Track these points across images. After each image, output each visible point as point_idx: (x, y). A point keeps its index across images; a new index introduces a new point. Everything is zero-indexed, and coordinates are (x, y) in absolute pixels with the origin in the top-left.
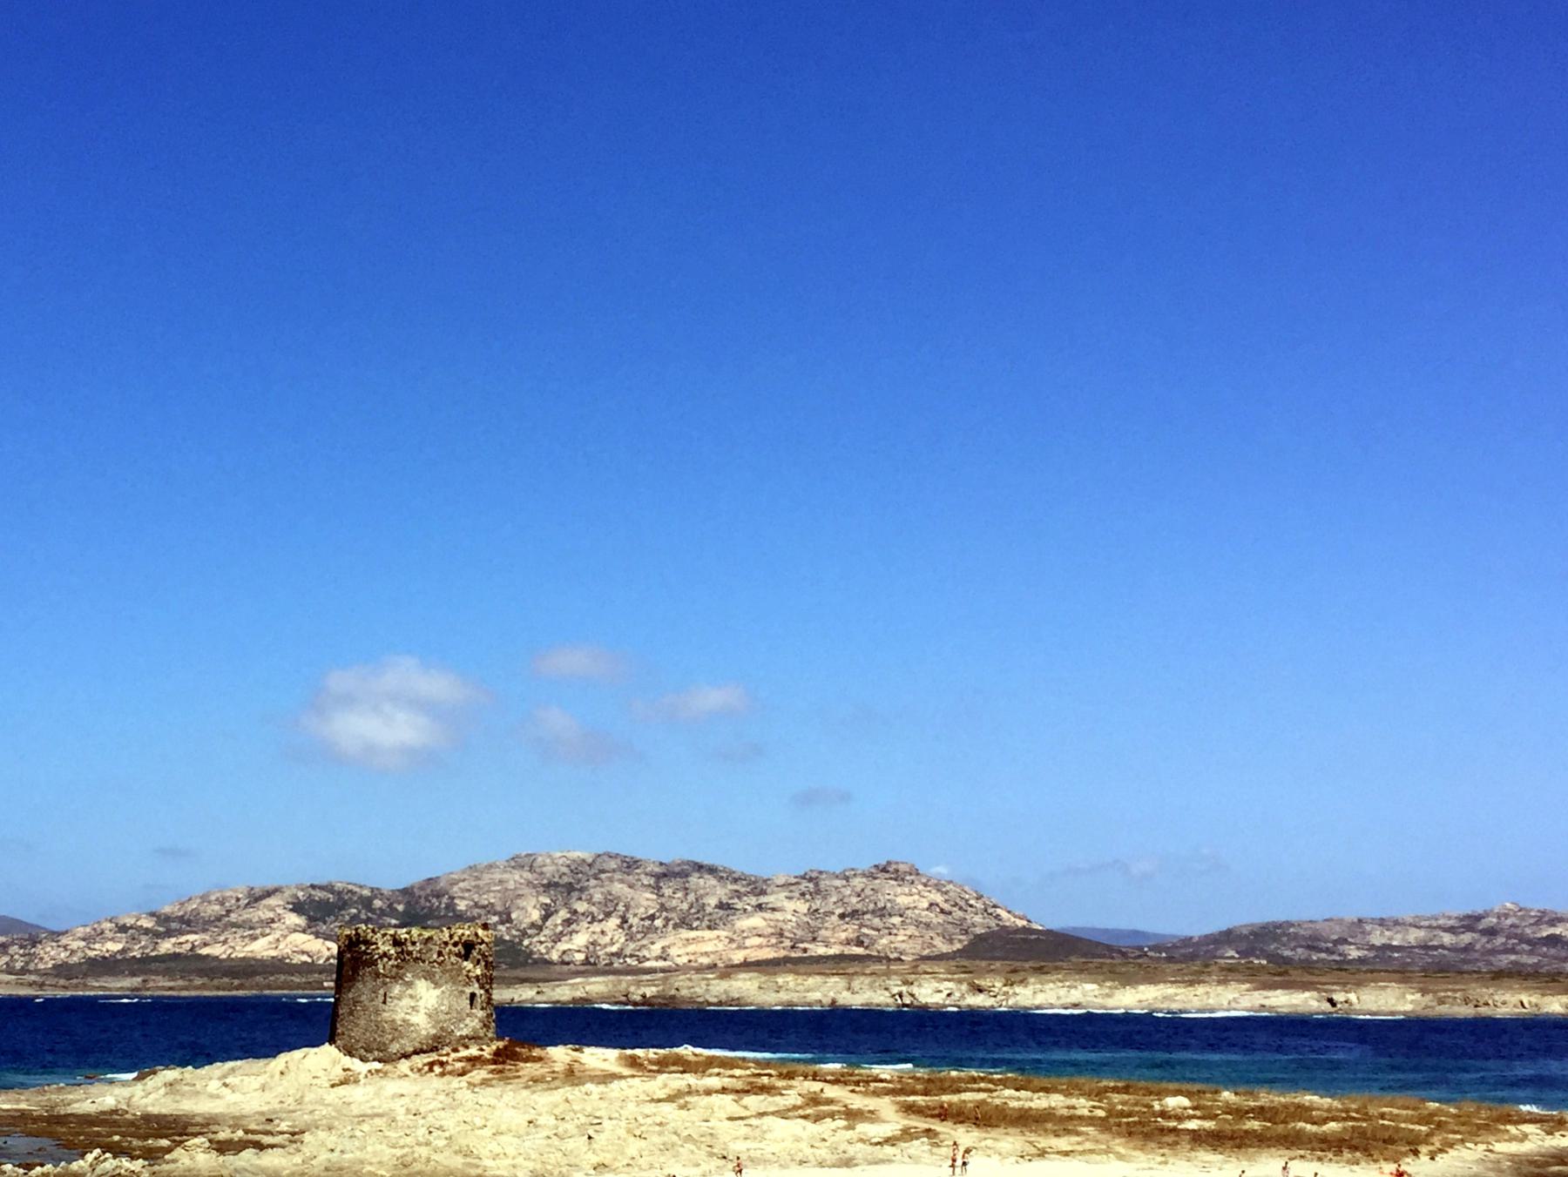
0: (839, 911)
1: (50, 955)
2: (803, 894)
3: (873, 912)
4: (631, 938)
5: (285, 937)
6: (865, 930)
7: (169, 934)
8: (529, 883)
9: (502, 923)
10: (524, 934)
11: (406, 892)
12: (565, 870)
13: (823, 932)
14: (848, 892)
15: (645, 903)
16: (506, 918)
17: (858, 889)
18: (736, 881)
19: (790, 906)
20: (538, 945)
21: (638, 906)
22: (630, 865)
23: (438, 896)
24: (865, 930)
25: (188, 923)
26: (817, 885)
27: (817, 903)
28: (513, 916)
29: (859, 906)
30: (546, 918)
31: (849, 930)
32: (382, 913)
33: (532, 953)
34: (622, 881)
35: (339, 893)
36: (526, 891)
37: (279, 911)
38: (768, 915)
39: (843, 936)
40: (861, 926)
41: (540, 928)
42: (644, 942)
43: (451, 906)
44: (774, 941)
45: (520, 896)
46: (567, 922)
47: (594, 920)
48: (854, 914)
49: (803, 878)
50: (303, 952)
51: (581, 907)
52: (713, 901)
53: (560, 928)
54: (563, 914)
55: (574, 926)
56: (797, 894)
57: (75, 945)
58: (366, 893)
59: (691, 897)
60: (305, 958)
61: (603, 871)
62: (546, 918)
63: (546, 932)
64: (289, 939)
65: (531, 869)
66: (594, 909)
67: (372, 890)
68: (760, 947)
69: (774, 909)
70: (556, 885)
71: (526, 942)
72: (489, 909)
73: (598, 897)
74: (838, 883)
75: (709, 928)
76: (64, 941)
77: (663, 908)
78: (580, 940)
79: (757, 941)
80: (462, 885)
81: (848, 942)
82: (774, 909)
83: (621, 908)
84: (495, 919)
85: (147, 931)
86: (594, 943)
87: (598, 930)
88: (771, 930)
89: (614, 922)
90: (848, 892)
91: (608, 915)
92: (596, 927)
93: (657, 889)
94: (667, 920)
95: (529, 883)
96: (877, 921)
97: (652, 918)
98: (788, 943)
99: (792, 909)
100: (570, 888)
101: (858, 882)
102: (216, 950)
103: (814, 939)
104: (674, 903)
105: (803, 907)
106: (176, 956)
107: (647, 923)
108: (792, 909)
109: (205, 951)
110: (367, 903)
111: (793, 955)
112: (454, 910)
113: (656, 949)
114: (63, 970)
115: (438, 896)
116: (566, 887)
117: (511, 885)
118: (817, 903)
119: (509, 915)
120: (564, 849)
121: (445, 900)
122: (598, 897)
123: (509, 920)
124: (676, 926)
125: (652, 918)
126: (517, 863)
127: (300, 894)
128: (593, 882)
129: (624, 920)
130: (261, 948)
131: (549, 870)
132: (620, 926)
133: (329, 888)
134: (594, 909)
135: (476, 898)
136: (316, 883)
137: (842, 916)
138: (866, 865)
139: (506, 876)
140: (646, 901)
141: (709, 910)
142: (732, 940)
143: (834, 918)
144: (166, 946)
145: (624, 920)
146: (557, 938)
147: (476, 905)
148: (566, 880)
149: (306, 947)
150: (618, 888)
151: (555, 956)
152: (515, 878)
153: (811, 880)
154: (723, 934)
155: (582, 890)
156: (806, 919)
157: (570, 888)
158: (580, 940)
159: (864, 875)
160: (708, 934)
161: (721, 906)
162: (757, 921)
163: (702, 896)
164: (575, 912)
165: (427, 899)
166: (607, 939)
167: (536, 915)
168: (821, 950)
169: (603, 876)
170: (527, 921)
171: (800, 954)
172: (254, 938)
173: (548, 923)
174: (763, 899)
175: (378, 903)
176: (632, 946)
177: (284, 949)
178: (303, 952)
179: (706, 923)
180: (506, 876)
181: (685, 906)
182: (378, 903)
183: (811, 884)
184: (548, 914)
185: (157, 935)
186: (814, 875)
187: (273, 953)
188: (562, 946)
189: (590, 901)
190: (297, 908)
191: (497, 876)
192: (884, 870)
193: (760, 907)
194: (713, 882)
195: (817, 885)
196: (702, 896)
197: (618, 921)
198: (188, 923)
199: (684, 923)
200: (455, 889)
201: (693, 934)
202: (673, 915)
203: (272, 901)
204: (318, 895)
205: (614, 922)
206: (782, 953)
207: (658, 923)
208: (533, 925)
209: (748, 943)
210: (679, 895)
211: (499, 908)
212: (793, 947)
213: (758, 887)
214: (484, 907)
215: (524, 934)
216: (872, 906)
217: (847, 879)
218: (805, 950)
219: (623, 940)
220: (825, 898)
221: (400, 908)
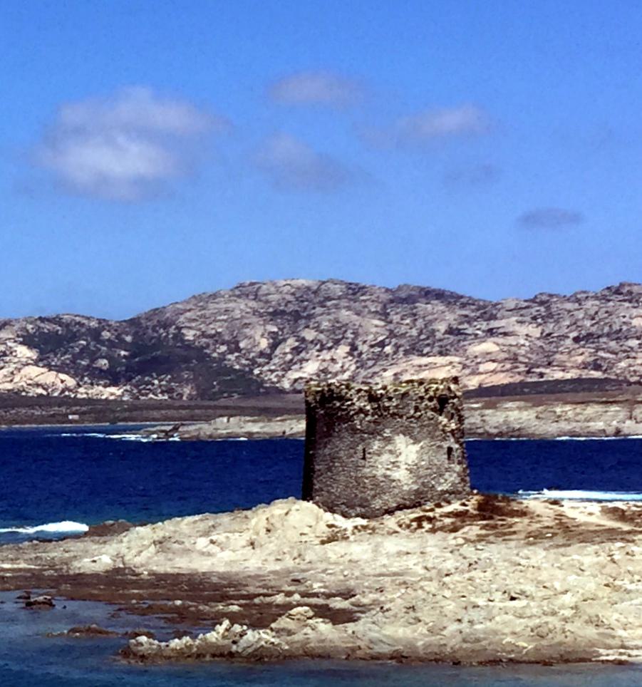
0: (575, 334)
2: (534, 318)
3: (608, 335)
4: (361, 365)
5: (19, 370)
6: (601, 354)
8: (255, 312)
9: (231, 352)
10: (254, 363)
11: (134, 322)
12: (289, 298)
13: (558, 356)
14: (580, 315)
15: (374, 330)
17: (592, 312)
18: (463, 306)
19: (523, 330)
20: (268, 374)
21: (367, 334)
22: (355, 291)
23: (166, 326)
24: (601, 354)
26: (548, 308)
27: (550, 327)
28: (242, 345)
29: (593, 329)
30: (274, 347)
31: (584, 354)
32: (110, 344)
33: (263, 381)
34: (348, 308)
35: (68, 325)
36: (254, 319)
37: (10, 344)
38: (501, 340)
39: (580, 359)
40: (598, 349)
41: (269, 357)
42: (376, 369)
43: (179, 336)
44: (508, 366)
45: (246, 325)
46: (296, 350)
48: (590, 335)
49: (533, 301)
50: (38, 385)
51: (309, 335)
52: (442, 327)
53: (289, 357)
54: (292, 342)
55: (303, 355)
56: (528, 319)
58: (93, 324)
59: (420, 323)
60: (40, 391)
61: (329, 299)
62: (274, 347)
63: (276, 360)
64: (23, 372)
65: (256, 298)
66: (322, 336)
67: (100, 321)
68: (494, 372)
69: (505, 334)
70: (283, 312)
71: (256, 371)
73: (325, 325)
74: (569, 306)
75: (441, 354)
77: (392, 334)
78: (311, 368)
79: (492, 366)
80: (188, 315)
81: (585, 366)
82: (505, 334)
83: (349, 335)
84: (223, 348)
86: (325, 371)
87: (328, 357)
88: (506, 355)
89: (343, 350)
90: (580, 315)
91: (337, 343)
92: (326, 355)
93: (384, 315)
94: (397, 347)
95: (255, 312)
96: (613, 344)
97: (382, 344)
98: (522, 368)
99: (525, 334)
100: (296, 316)
101: (591, 305)
103: (549, 364)
104: (403, 329)
105: (535, 331)
107: (377, 349)
108: (525, 334)
110: (95, 334)
111: (529, 380)
112: (183, 341)
113: (389, 375)
115: (166, 326)
116: (293, 314)
117: (237, 314)
118: (550, 327)
119: (237, 343)
120: (290, 274)
121: (172, 330)
123: (238, 349)
124: (406, 353)
125: (382, 344)
126: (245, 291)
127: (30, 327)
128: (319, 310)
129: (354, 348)
131: (274, 298)
132: (350, 354)
133: (56, 320)
134: (322, 336)
135: (203, 327)
136: (43, 316)
137: (576, 340)
138: (598, 287)
139: (231, 305)
140: (374, 327)
141: (439, 335)
142: (465, 367)
143: (569, 342)
145: (354, 348)
146: (288, 366)
147: (204, 335)
148: (291, 308)
149: (41, 380)
150: (345, 315)
151: (286, 385)
152: (241, 307)
153: (542, 303)
154: (457, 359)
155: (310, 317)
156: (539, 343)
157: (296, 316)
158: (311, 368)
159: (596, 298)
160: (440, 360)
161: (450, 331)
162: (489, 346)
163: (431, 322)
164: (303, 340)
165: (154, 330)
166: (337, 367)
167: (264, 344)
168: (559, 375)
169: (329, 303)
170: (257, 349)
171: (535, 379)
173: (277, 352)
174: (494, 324)
175: (106, 335)
176: (363, 373)
177: (20, 381)
178: (38, 385)
179: (436, 349)
180: (231, 305)
181: (414, 332)
182: (106, 335)
183: (542, 308)
186: (544, 298)
187: (9, 386)
189: (317, 329)
190: (28, 341)
191: (223, 306)
192: (618, 292)
193: (491, 332)
194: (442, 307)
195: (548, 308)
196: (431, 322)
197: (347, 349)
199: (415, 349)
200: (182, 319)
201: (425, 360)
202: (403, 341)
204: (47, 327)
205: (343, 350)
206: (518, 379)
207: (388, 349)
208: (262, 354)
209: (482, 368)
210: (408, 321)
211: (227, 338)
212: (528, 372)
213: (487, 312)
214: (212, 336)
215: (254, 363)
216: (606, 329)
217: (578, 301)
218: (541, 375)
219: (353, 368)
220: (557, 322)
221: (129, 339)
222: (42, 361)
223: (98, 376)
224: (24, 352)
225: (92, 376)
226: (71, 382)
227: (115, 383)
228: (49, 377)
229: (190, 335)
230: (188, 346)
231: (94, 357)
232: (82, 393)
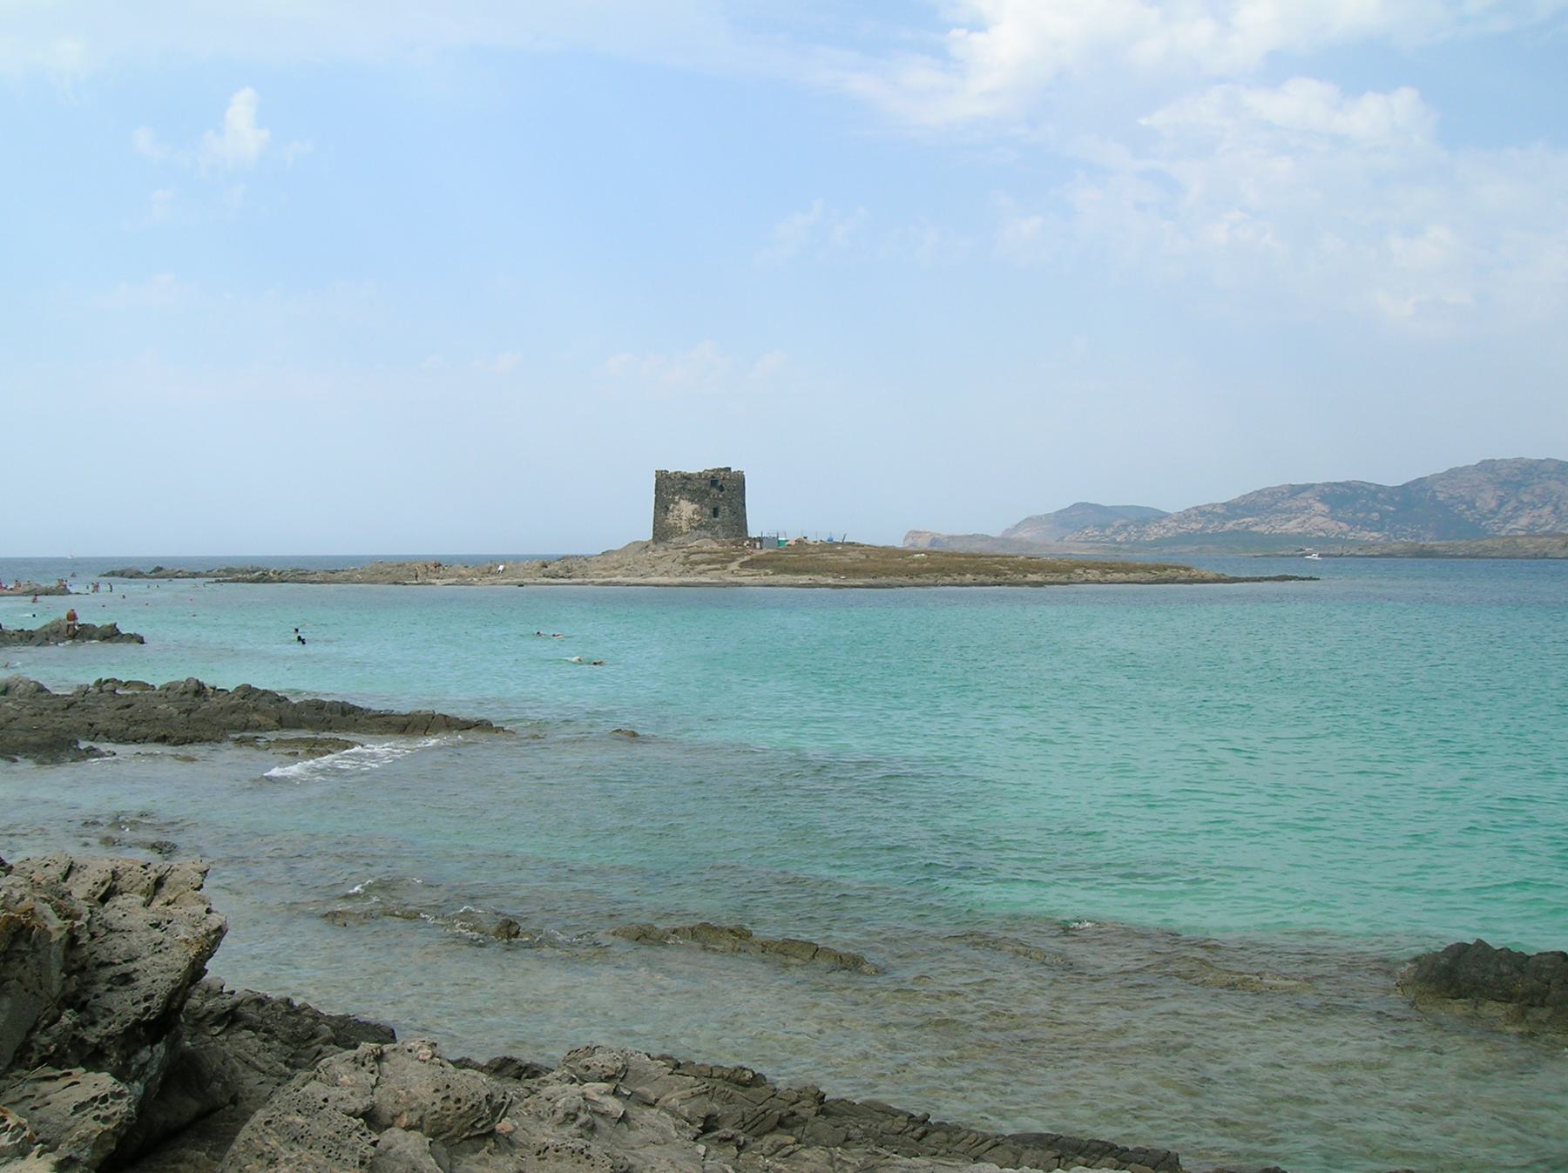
1: (1154, 532)
10: (1484, 517)
16: (1471, 505)
30: (1500, 506)
46: (1515, 509)
47: (1535, 507)
51: (1526, 498)
54: (1513, 503)
57: (1170, 525)
62: (1500, 506)
76: (1165, 522)
78: (1524, 521)
85: (1219, 515)
89: (1548, 509)
91: (1545, 504)
102: (1262, 528)
114: (1160, 542)
123: (1474, 507)
130: (1292, 527)
144: (1230, 525)
146: (1506, 521)
147: (1452, 497)
150: (1553, 485)
167: (1493, 504)
184: (1502, 503)
188: (1510, 526)
190: (1323, 499)
205: (1548, 509)
208: (1491, 511)
215: (1484, 517)
224: (1319, 507)
226: (1345, 527)
228: (1331, 525)
229: (1441, 497)
232: (1351, 535)
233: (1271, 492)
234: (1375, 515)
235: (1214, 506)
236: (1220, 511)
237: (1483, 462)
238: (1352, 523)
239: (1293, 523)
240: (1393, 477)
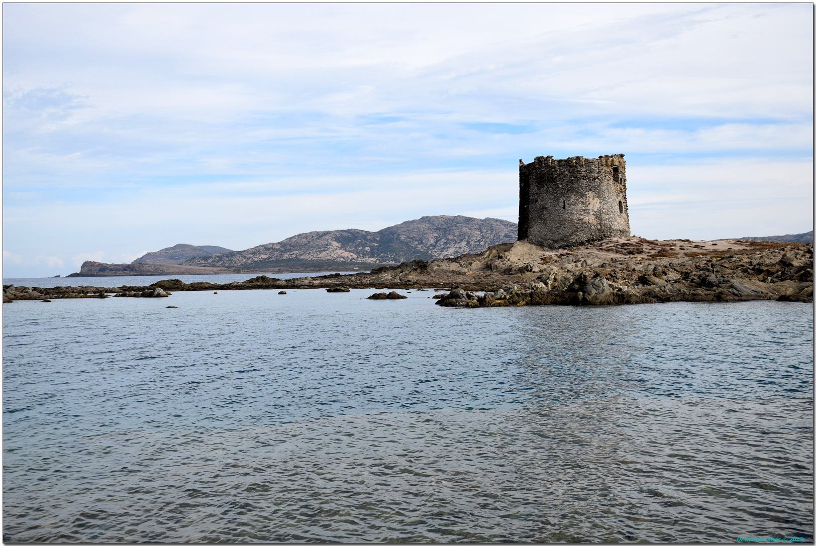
7: (286, 251)
23: (393, 234)
25: (293, 246)
32: (371, 241)
51: (451, 237)
54: (444, 240)
62: (436, 242)
72: (413, 239)
73: (457, 233)
85: (277, 250)
89: (464, 243)
91: (462, 240)
93: (480, 230)
106: (289, 260)
109: (302, 257)
115: (393, 234)
122: (457, 233)
123: (422, 243)
125: (479, 241)
129: (468, 243)
167: (432, 241)
172: (321, 252)
175: (369, 237)
177: (334, 256)
182: (369, 237)
184: (437, 240)
185: (282, 251)
190: (337, 240)
198: (293, 246)
203: (327, 237)
205: (464, 243)
207: (482, 243)
222: (343, 247)
223: (365, 254)
224: (336, 244)
225: (363, 254)
226: (355, 256)
227: (372, 257)
228: (346, 254)
229: (403, 238)
230: (402, 242)
231: (364, 246)
232: (359, 260)
233: (306, 236)
234: (367, 249)
235: (273, 244)
236: (277, 247)
237: (423, 218)
238: (358, 253)
239: (324, 253)
240: (374, 227)
